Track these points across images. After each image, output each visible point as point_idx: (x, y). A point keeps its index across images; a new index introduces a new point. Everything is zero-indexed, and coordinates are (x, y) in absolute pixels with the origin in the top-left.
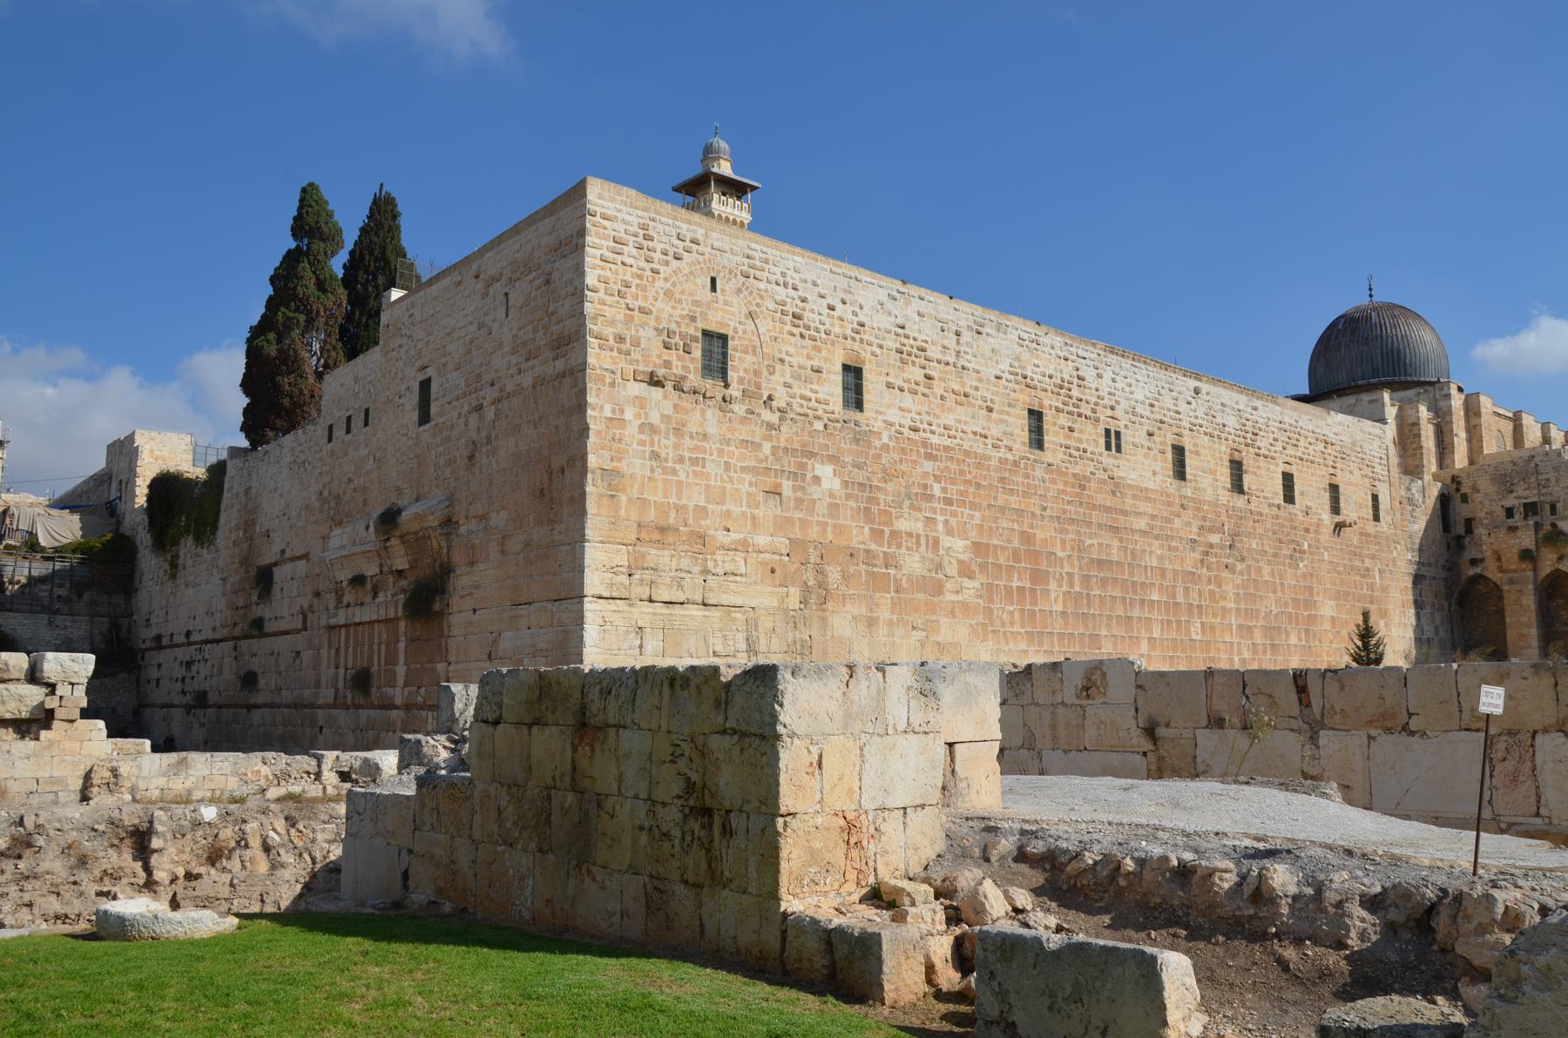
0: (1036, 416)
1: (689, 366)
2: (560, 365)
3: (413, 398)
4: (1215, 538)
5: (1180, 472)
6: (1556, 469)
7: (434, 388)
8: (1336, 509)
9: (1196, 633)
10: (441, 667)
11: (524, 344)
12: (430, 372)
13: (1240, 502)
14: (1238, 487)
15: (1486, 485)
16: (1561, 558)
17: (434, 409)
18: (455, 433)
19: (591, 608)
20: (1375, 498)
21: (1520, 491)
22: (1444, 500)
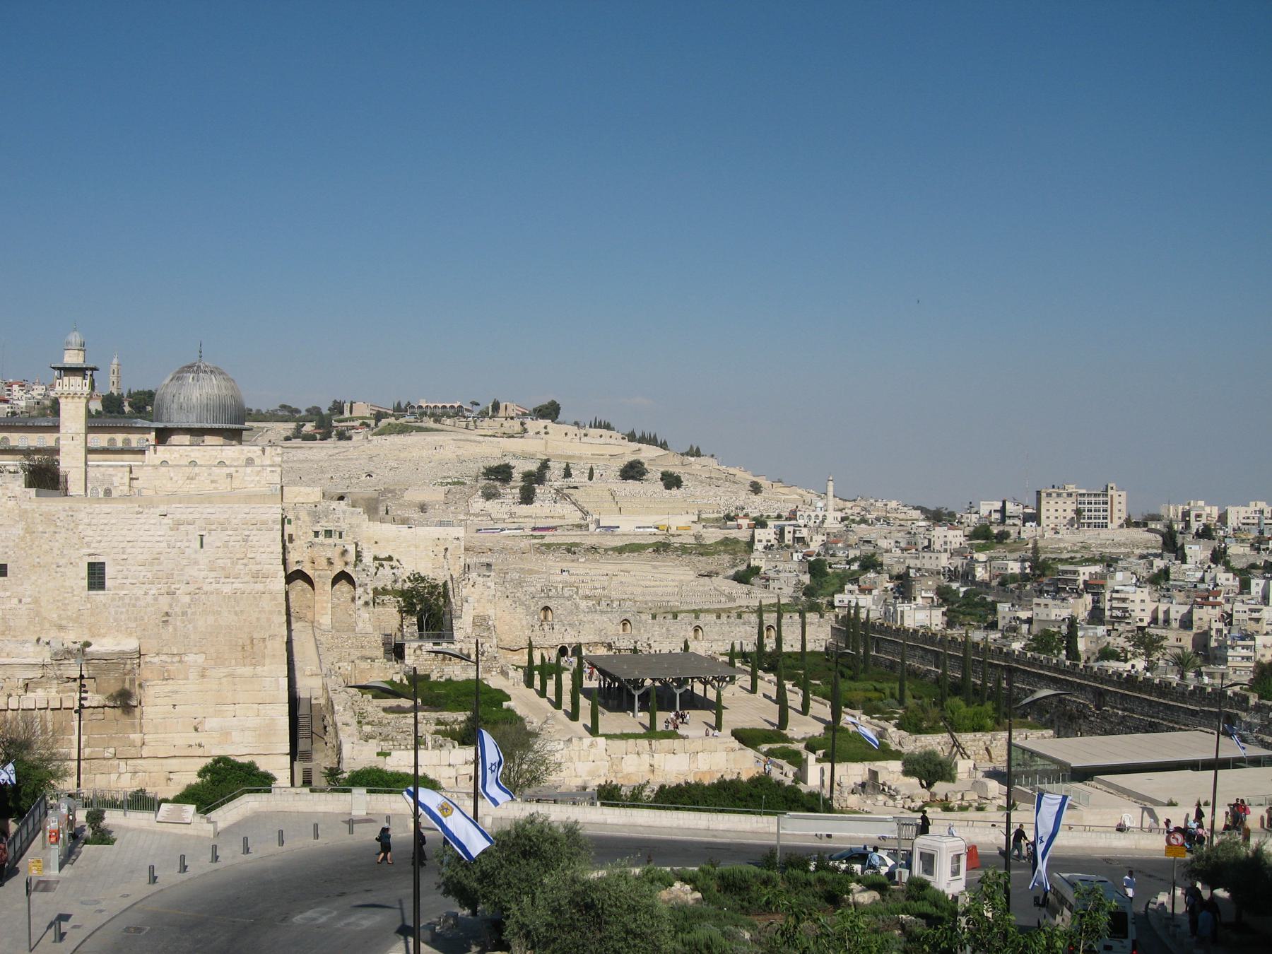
2: (259, 587)
3: (85, 573)
6: (344, 513)
7: (109, 571)
10: (136, 737)
11: (223, 568)
12: (101, 559)
15: (303, 515)
16: (346, 564)
17: (108, 583)
18: (142, 603)
21: (323, 522)
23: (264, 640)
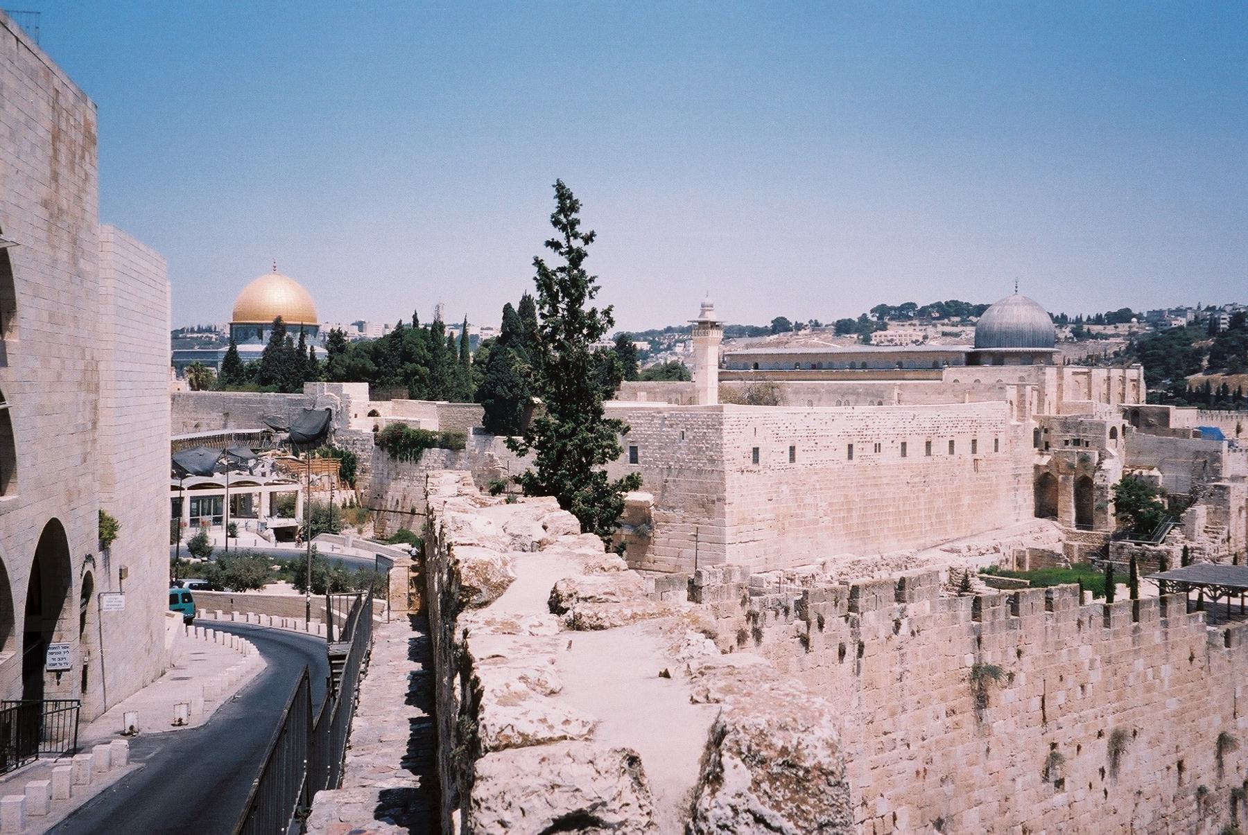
0: (850, 447)
1: (749, 462)
4: (917, 480)
5: (904, 454)
8: (974, 451)
9: (907, 523)
13: (929, 459)
14: (928, 452)
19: (727, 547)
20: (996, 440)
22: (1036, 433)
23: (713, 502)
